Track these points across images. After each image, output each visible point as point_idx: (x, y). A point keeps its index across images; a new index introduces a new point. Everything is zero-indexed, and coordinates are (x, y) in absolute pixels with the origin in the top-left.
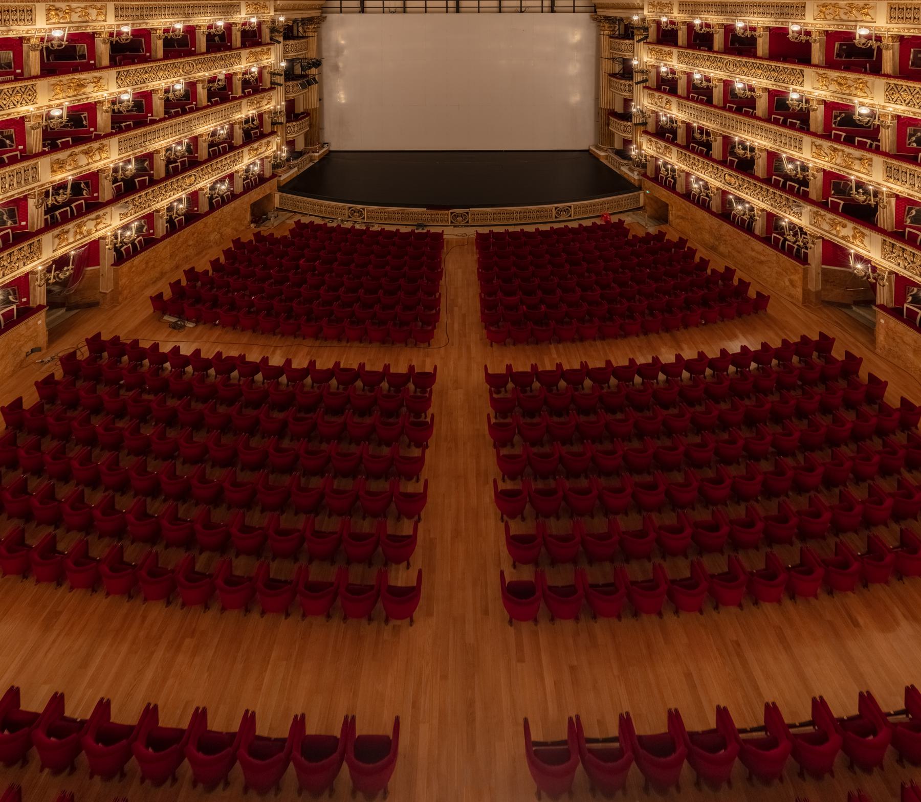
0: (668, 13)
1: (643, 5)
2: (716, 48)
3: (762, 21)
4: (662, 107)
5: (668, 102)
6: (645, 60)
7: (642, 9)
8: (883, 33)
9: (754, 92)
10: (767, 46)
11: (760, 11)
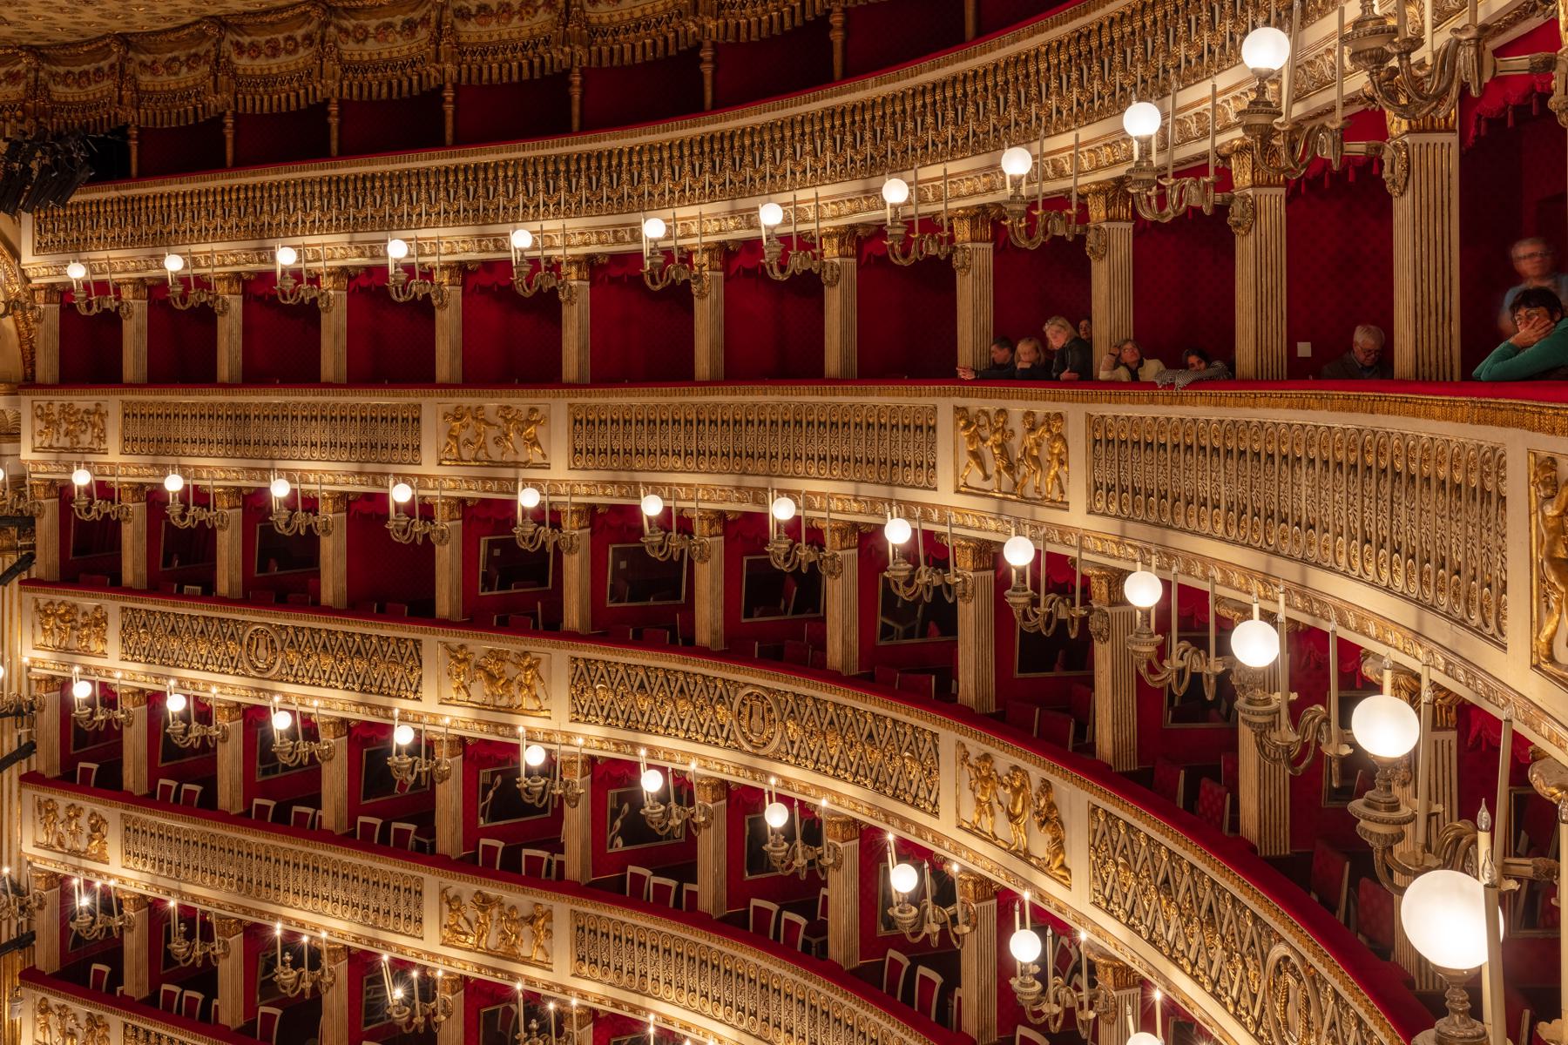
0: (92, 451)
1: (18, 417)
2: (222, 587)
3: (330, 472)
4: (75, 853)
5: (97, 827)
6: (26, 660)
7: (14, 435)
8: (564, 500)
9: (317, 740)
10: (342, 566)
11: (326, 437)
